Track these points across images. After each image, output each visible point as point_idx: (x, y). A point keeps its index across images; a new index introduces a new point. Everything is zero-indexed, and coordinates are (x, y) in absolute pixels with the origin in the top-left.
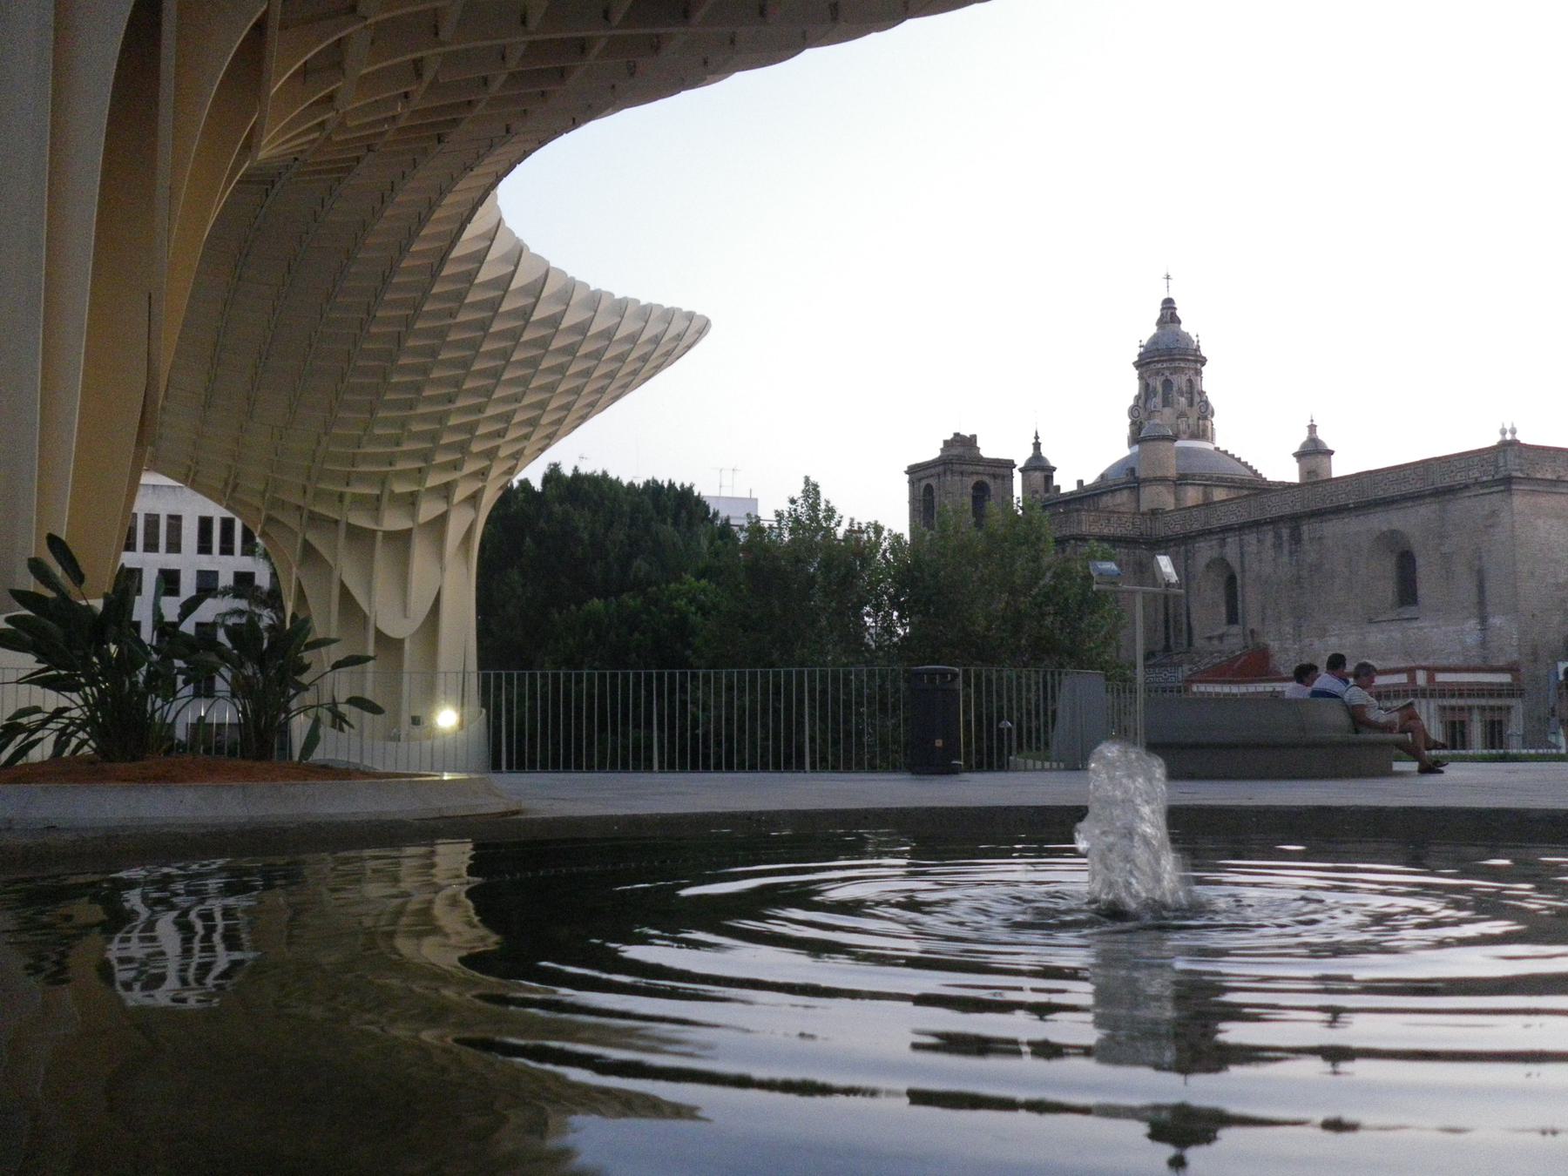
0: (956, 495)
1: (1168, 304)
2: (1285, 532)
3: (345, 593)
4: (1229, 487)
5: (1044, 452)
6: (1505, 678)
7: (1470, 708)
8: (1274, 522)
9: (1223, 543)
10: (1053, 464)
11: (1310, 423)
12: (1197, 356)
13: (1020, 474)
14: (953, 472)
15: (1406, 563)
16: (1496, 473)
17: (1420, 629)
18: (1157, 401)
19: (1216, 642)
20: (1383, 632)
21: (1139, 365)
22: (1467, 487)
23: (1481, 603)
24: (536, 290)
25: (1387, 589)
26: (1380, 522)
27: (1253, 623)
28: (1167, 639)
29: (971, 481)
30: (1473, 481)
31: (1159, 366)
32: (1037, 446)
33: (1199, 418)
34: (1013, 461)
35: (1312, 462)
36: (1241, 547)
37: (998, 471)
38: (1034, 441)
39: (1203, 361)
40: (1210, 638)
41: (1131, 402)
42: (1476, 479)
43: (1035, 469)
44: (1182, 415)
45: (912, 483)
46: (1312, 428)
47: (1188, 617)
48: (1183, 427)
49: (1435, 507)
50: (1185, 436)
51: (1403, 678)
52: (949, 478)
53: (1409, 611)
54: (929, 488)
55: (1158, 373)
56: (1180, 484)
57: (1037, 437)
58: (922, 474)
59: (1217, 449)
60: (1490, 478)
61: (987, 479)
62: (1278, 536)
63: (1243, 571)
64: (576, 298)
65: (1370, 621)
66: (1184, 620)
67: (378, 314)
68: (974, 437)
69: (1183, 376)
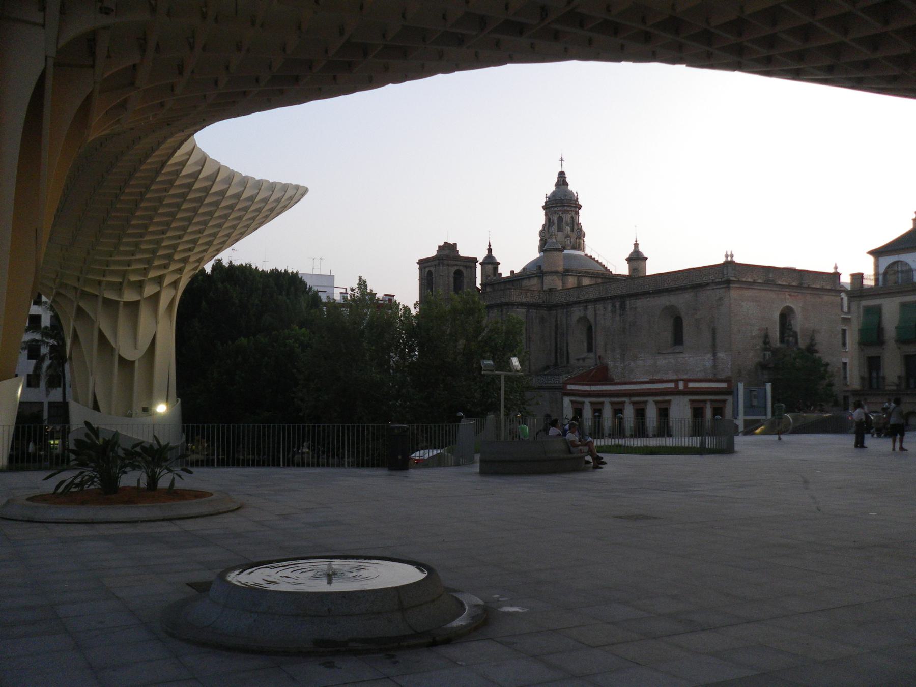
0: (446, 275)
1: (562, 175)
2: (618, 304)
3: (101, 336)
4: (591, 277)
5: (494, 254)
6: (724, 385)
7: (705, 401)
8: (612, 298)
9: (586, 309)
12: (576, 204)
13: (480, 266)
14: (443, 265)
15: (678, 323)
16: (723, 277)
17: (683, 358)
18: (554, 229)
19: (581, 362)
20: (665, 359)
21: (545, 208)
22: (708, 284)
23: (714, 346)
24: (213, 178)
25: (668, 336)
27: (600, 352)
28: (556, 358)
29: (454, 269)
30: (711, 281)
31: (556, 209)
32: (490, 250)
33: (576, 238)
34: (476, 259)
35: (635, 264)
36: (595, 311)
37: (468, 264)
38: (488, 247)
39: (580, 207)
40: (578, 360)
41: (541, 228)
42: (713, 280)
43: (488, 263)
44: (567, 236)
45: (420, 269)
46: (636, 245)
47: (567, 346)
48: (568, 242)
49: (692, 294)
50: (569, 248)
51: (672, 385)
52: (441, 268)
53: (678, 348)
54: (430, 273)
55: (555, 212)
56: (565, 275)
57: (490, 246)
58: (426, 264)
59: (586, 255)
60: (720, 280)
61: (461, 268)
62: (614, 306)
63: (596, 324)
64: (235, 180)
65: (659, 353)
66: (565, 349)
67: (126, 191)
68: (455, 245)
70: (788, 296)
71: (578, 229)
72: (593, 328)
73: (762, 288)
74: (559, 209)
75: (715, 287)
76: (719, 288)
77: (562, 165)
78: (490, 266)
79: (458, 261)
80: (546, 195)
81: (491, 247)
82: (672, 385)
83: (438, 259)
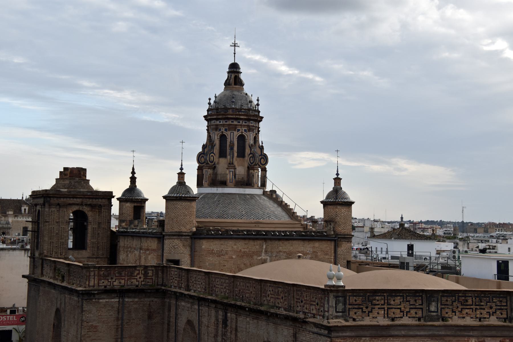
1: (234, 68)
5: (139, 185)
10: (146, 197)
11: (336, 176)
13: (118, 202)
31: (218, 122)
32: (133, 179)
38: (131, 175)
46: (337, 180)
48: (229, 176)
52: (47, 210)
55: (217, 128)
56: (195, 238)
57: (133, 173)
61: (86, 209)
69: (236, 133)
71: (251, 153)
73: (411, 333)
74: (221, 123)
75: (315, 330)
76: (320, 335)
77: (235, 54)
78: (128, 204)
79: (76, 198)
80: (210, 99)
81: (135, 175)
83: (44, 197)
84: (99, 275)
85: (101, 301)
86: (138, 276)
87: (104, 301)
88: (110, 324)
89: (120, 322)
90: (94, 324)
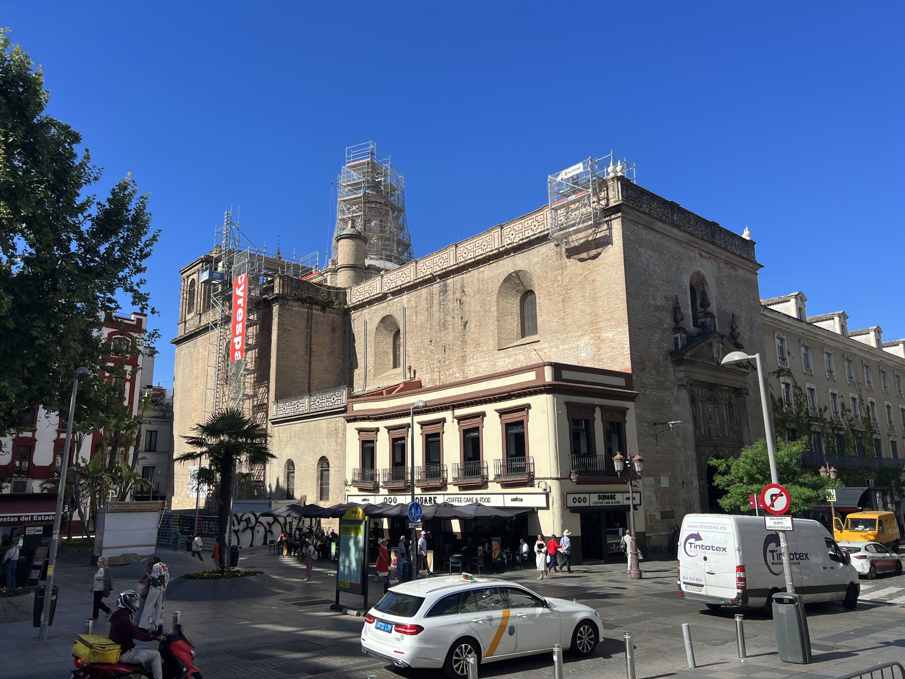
7: (592, 407)
15: (527, 296)
26: (507, 266)
27: (411, 361)
70: (698, 256)
72: (401, 331)
82: (531, 376)
84: (291, 287)
85: (293, 308)
86: (323, 294)
87: (296, 309)
88: (301, 330)
89: (309, 330)
90: (288, 327)
